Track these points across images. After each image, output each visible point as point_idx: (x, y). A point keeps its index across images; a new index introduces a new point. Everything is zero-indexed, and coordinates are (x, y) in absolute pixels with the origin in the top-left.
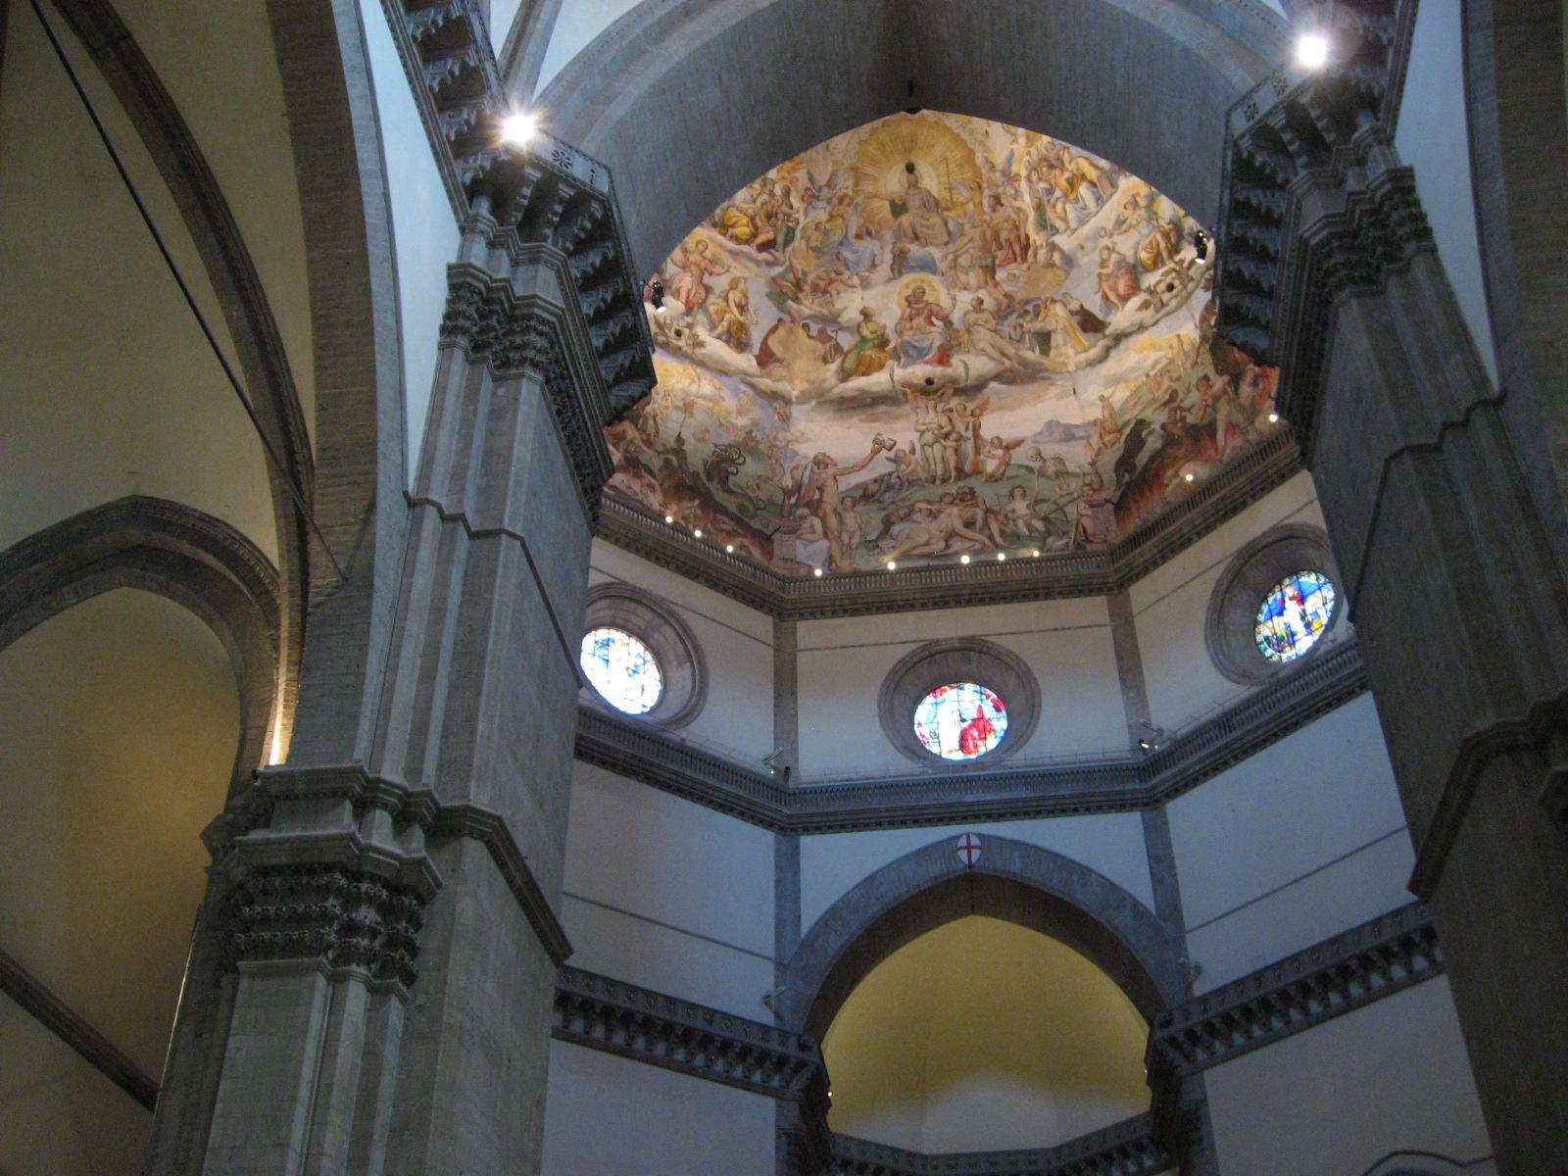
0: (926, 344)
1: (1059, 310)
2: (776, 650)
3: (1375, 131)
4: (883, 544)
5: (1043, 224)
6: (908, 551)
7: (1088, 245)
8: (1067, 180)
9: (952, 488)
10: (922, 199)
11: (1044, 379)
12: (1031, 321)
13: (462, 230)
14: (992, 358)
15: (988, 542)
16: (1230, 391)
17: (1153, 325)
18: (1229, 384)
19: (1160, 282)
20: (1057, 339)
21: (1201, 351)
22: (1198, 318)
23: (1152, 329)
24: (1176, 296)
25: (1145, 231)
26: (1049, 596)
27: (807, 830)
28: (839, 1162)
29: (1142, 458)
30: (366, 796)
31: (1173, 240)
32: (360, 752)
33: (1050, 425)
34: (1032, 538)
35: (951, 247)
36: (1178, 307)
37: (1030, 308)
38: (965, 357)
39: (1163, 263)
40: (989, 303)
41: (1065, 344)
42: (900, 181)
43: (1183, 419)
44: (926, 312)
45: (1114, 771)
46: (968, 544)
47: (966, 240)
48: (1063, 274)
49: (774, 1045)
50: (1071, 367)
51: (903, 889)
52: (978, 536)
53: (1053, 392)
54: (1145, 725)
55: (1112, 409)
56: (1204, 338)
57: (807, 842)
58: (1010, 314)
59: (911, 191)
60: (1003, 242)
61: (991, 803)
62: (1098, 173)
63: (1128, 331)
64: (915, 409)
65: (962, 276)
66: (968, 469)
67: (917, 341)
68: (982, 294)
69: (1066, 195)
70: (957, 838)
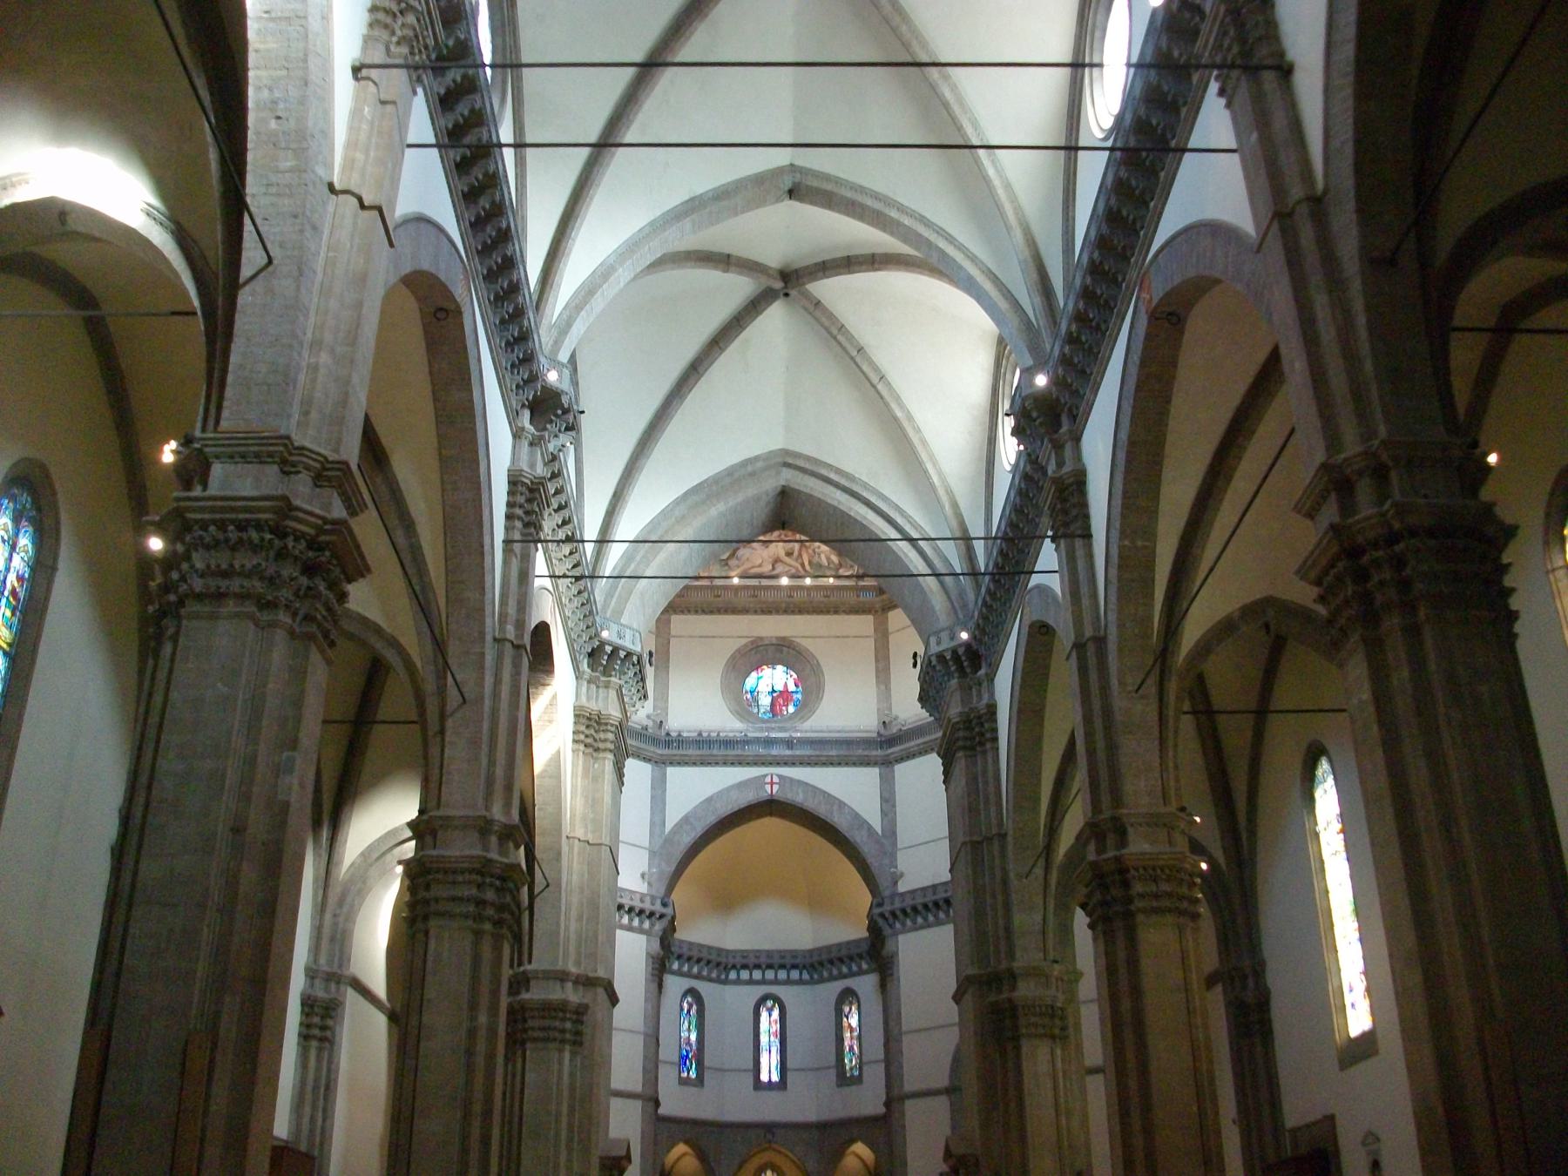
2: (657, 636)
3: (987, 674)
4: (730, 563)
6: (745, 571)
13: (577, 678)
15: (800, 568)
26: (836, 612)
27: (671, 764)
28: (676, 956)
30: (562, 977)
32: (560, 963)
45: (867, 742)
46: (787, 569)
49: (647, 906)
51: (730, 807)
52: (793, 563)
54: (887, 715)
57: (670, 770)
61: (788, 756)
70: (765, 776)
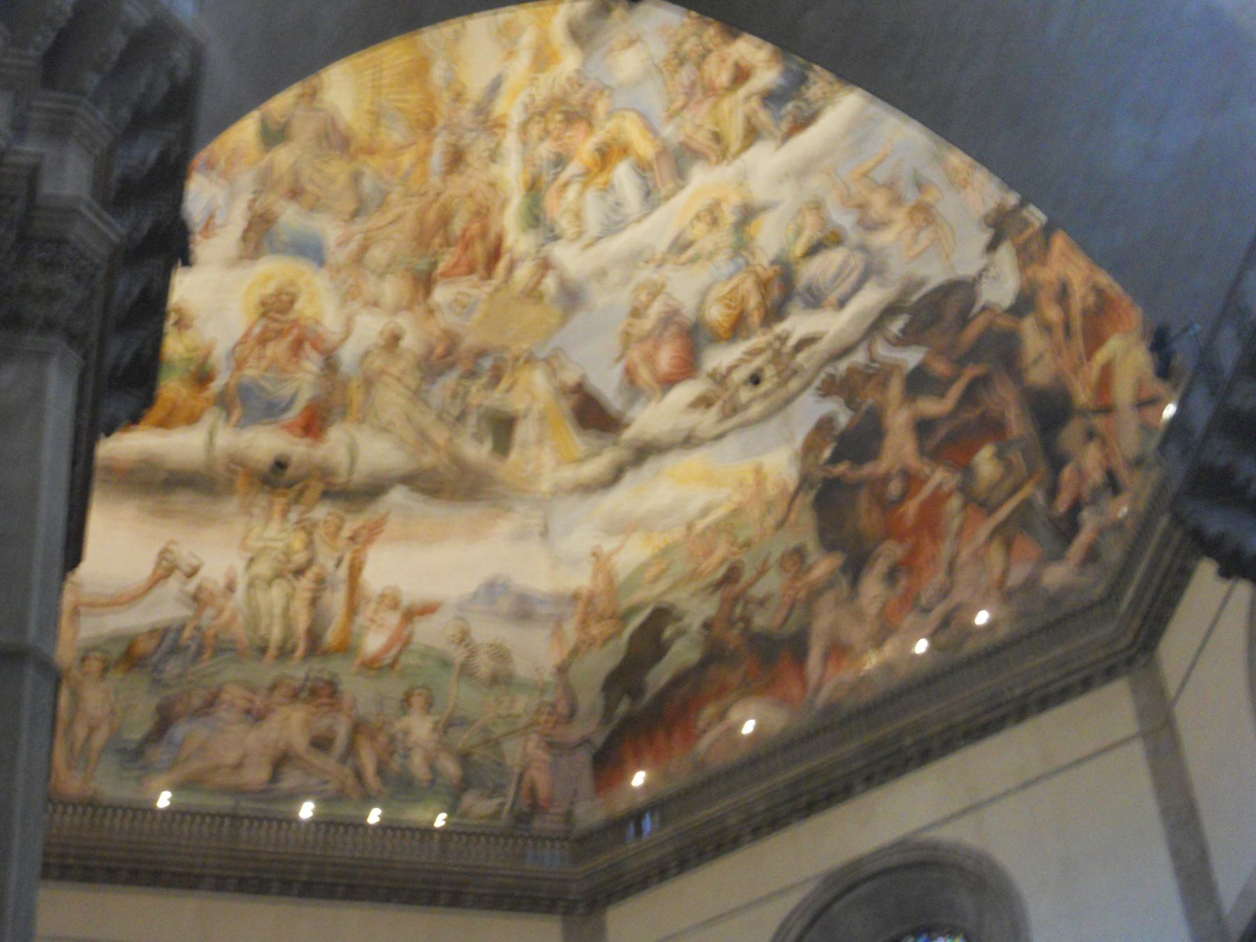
0: (286, 391)
1: (538, 380)
5: (535, 218)
7: (615, 275)
9: (297, 671)
18: (844, 569)
20: (525, 432)
21: (798, 501)
25: (722, 264)
29: (659, 676)
33: (492, 588)
34: (433, 789)
36: (765, 417)
40: (411, 342)
41: (540, 441)
43: (747, 620)
47: (390, 216)
50: (545, 486)
53: (505, 526)
56: (805, 481)
64: (246, 511)
66: (331, 637)
68: (404, 322)
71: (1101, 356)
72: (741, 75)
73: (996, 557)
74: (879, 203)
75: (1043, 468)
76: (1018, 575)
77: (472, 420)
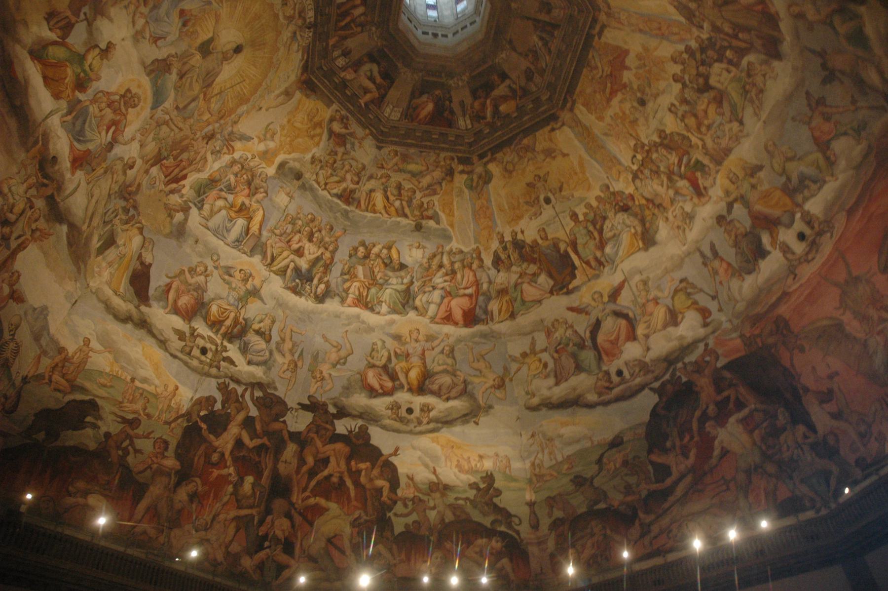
5: (201, 190)
7: (200, 247)
8: (243, 204)
10: (214, 69)
11: (79, 269)
12: (121, 219)
14: (87, 208)
16: (172, 482)
17: (172, 355)
18: (177, 472)
19: (203, 337)
21: (180, 420)
22: (197, 396)
23: (167, 354)
24: (201, 362)
31: (235, 330)
35: (175, 113)
36: (194, 370)
37: (132, 212)
38: (83, 183)
39: (217, 332)
41: (110, 264)
42: (229, 42)
43: (126, 452)
44: (118, 118)
47: (181, 125)
48: (167, 231)
53: (70, 286)
55: (84, 361)
56: (188, 415)
58: (126, 199)
59: (220, 56)
60: (179, 159)
62: (257, 233)
63: (155, 331)
65: (152, 135)
67: (91, 122)
68: (139, 162)
69: (232, 206)
71: (322, 502)
72: (299, 252)
73: (231, 530)
74: (288, 345)
75: (263, 507)
76: (235, 548)
77: (107, 229)
